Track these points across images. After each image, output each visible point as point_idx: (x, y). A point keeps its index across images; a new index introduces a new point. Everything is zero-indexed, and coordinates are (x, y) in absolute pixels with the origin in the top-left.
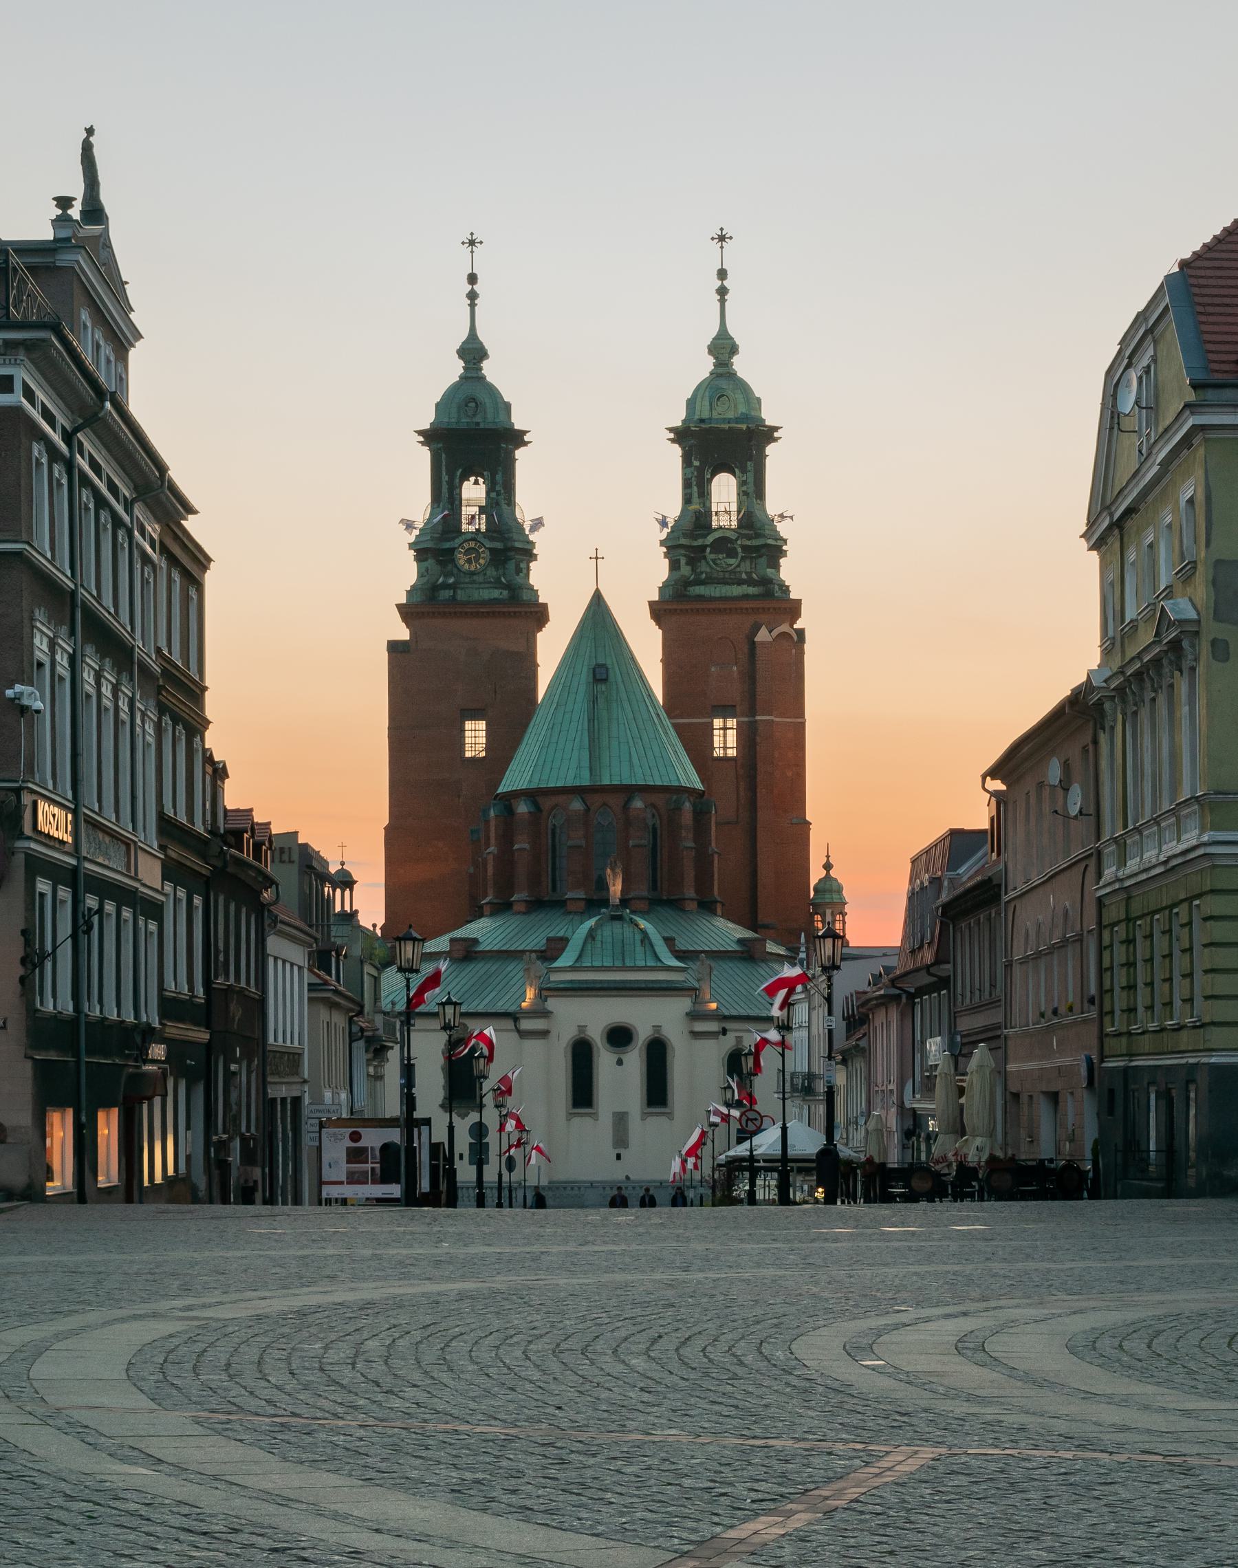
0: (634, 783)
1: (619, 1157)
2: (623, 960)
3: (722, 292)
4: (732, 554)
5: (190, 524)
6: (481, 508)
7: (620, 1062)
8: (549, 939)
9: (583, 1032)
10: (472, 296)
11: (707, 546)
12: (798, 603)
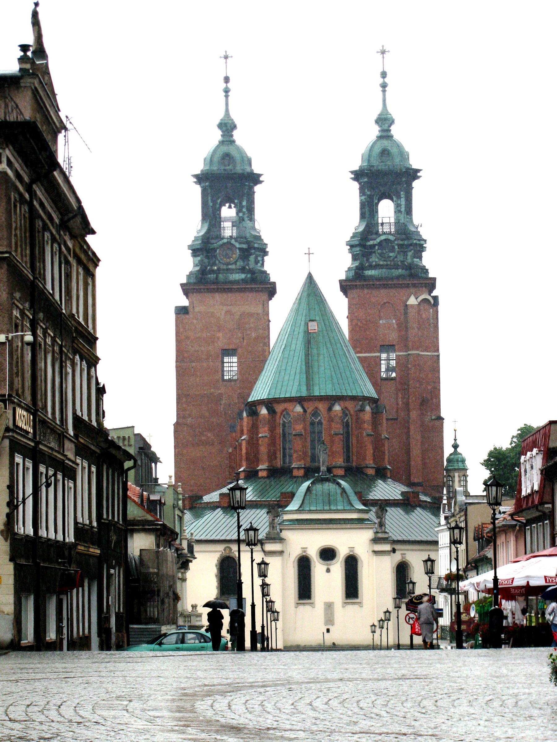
0: (334, 394)
1: (328, 631)
2: (330, 506)
3: (384, 86)
4: (393, 250)
5: (89, 238)
6: (233, 222)
7: (328, 571)
8: (282, 493)
9: (305, 552)
11: (376, 245)
12: (434, 279)
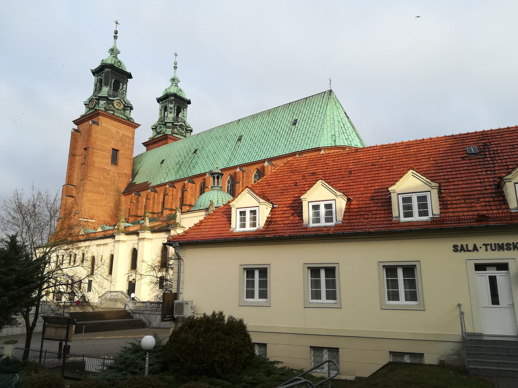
4: (183, 130)
11: (178, 125)
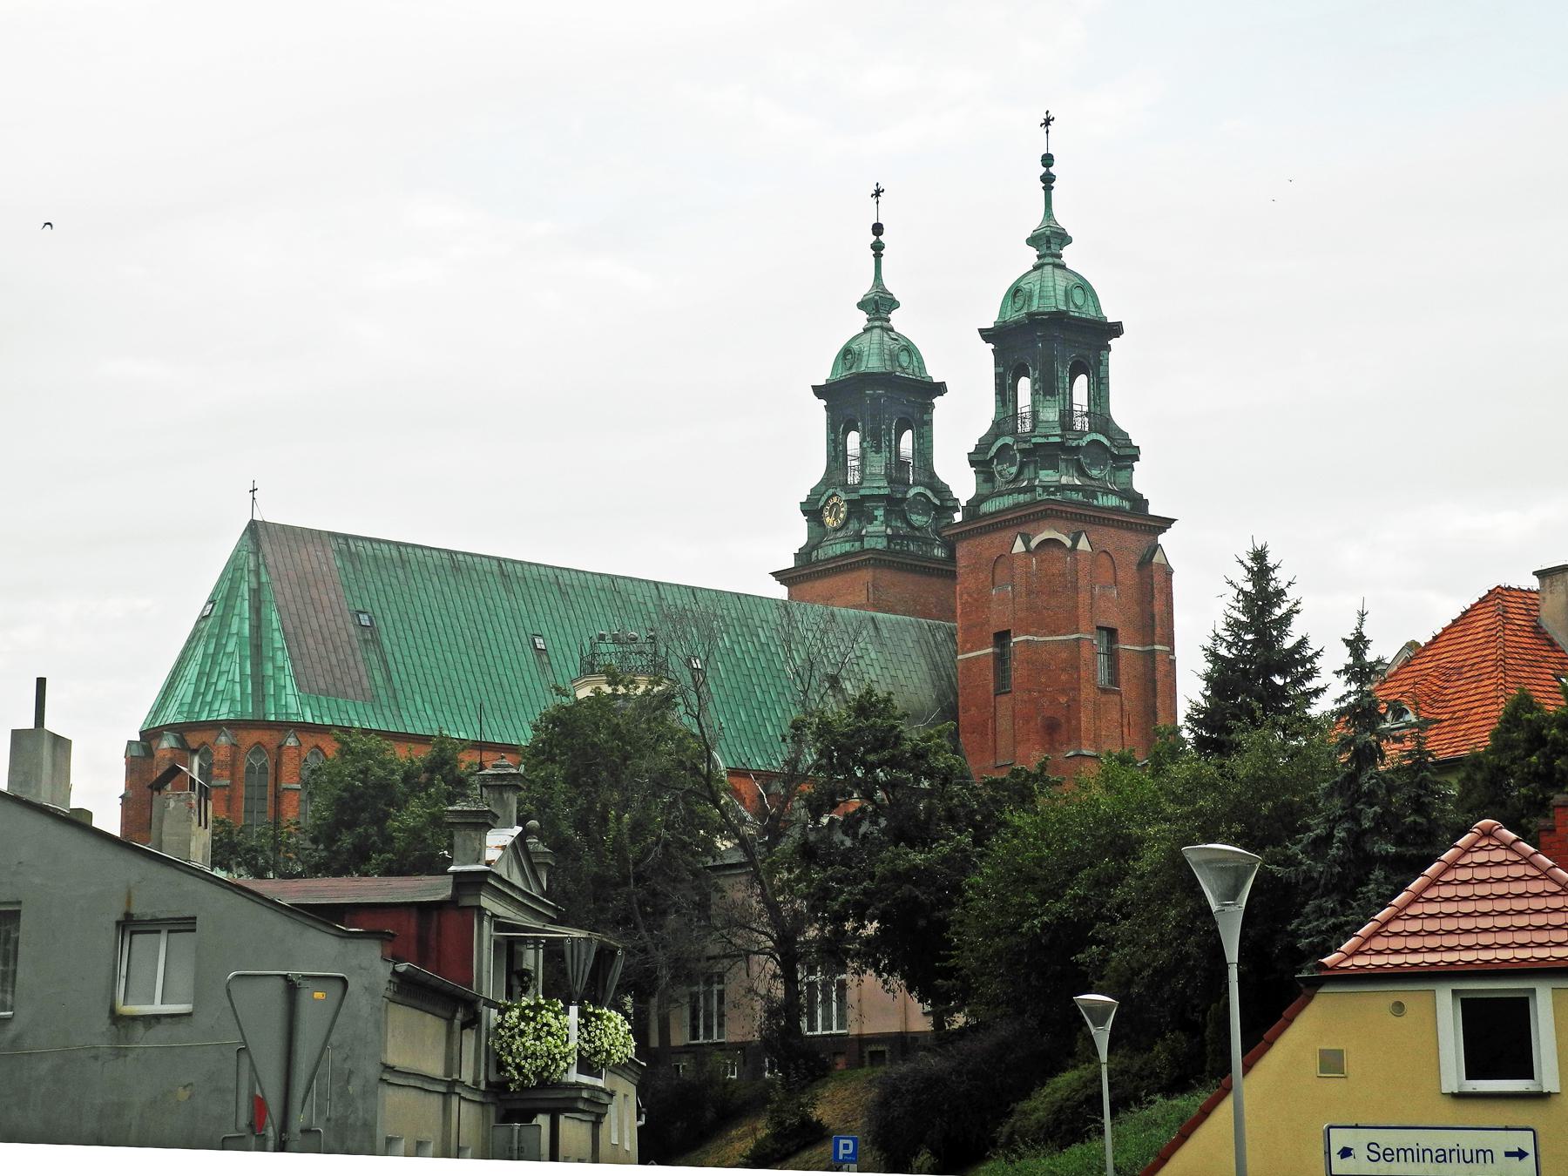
10: (878, 248)
